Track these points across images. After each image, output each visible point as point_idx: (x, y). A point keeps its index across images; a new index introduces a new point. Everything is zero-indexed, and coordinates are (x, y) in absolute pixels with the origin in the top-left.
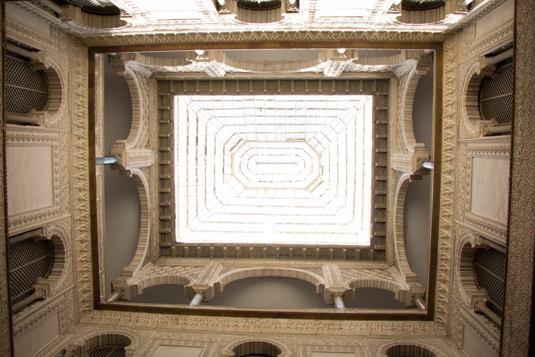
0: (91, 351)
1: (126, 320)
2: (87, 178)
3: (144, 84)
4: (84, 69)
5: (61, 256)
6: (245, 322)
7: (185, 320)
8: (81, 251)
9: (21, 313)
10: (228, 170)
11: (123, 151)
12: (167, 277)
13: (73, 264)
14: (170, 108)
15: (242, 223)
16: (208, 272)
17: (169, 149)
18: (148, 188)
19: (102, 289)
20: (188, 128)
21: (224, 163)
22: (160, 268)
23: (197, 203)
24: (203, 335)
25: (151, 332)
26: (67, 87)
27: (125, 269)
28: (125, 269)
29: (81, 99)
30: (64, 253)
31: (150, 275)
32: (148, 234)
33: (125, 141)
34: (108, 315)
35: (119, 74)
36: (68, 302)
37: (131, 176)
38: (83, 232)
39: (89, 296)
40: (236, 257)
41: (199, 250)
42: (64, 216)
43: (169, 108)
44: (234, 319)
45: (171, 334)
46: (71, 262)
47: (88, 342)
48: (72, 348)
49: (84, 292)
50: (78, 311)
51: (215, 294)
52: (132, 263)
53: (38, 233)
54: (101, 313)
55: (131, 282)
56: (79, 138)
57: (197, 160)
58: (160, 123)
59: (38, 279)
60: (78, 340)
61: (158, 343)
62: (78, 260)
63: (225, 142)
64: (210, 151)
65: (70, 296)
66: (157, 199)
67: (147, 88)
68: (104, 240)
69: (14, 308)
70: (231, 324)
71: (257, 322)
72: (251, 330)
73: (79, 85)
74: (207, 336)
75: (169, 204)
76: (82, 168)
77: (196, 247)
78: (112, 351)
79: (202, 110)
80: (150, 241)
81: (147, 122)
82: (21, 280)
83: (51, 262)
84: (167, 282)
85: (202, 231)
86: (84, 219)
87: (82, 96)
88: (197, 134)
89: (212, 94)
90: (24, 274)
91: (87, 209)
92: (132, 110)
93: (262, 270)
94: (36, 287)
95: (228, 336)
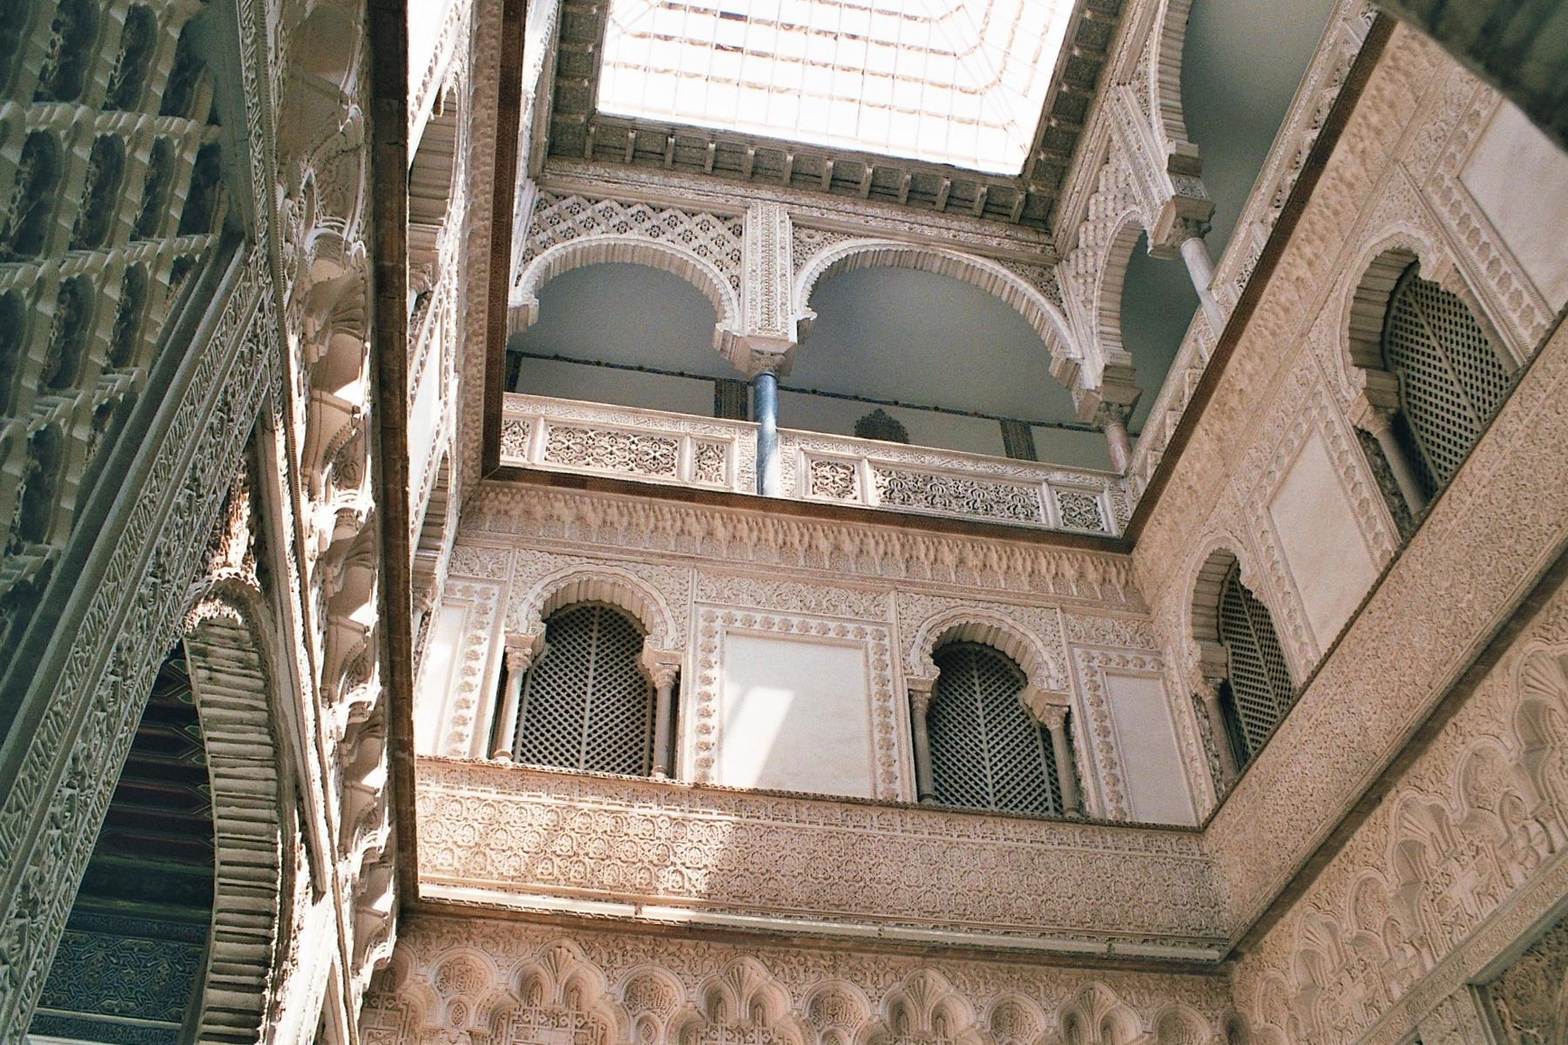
12: (1109, 264)
14: (633, 129)
18: (852, 242)
23: (920, 49)
27: (1054, 369)
28: (1054, 369)
33: (720, 327)
34: (1154, 535)
37: (814, 316)
41: (1059, 125)
42: (892, 616)
43: (632, 135)
47: (1199, 630)
53: (921, 706)
55: (1091, 377)
77: (1049, 128)
80: (998, 260)
83: (991, 654)
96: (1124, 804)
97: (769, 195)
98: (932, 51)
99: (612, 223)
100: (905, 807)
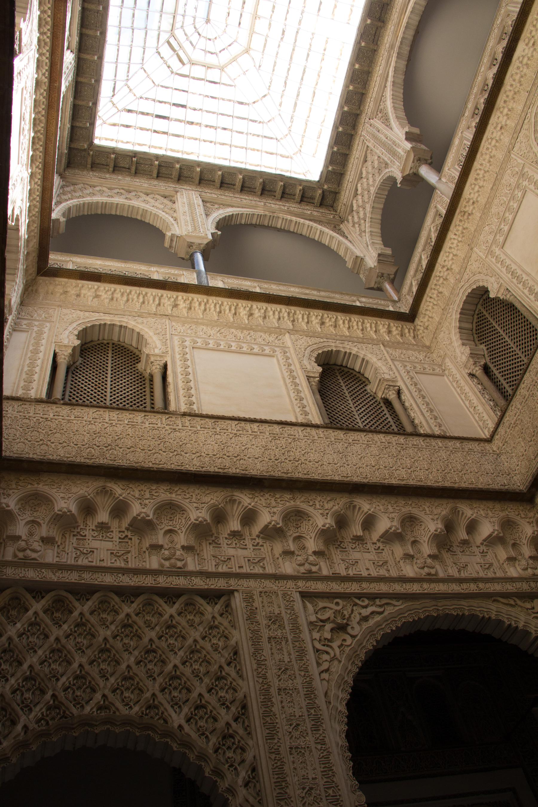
0: (476, 340)
1: (443, 283)
2: (235, 301)
3: (75, 192)
4: (73, 286)
5: (342, 355)
6: (501, 113)
7: (468, 202)
8: (335, 326)
9: (416, 421)
10: (213, 74)
11: (184, 240)
12: (373, 207)
13: (353, 342)
14: (113, 153)
15: (304, 70)
16: (383, 145)
17: (178, 166)
19: (380, 305)
20: (141, 129)
21: (202, 79)
22: (355, 214)
23: (258, 136)
24: (503, 181)
25: (474, 256)
26: (102, 314)
27: (349, 265)
28: (349, 265)
29: (117, 295)
30: (338, 352)
31: (365, 232)
32: (302, 221)
33: (169, 234)
35: (62, 229)
36: (402, 356)
37: (219, 233)
38: (310, 319)
39: (395, 326)
40: (363, 94)
41: (338, 150)
42: (289, 343)
43: (113, 156)
44: (490, 128)
45: (487, 228)
46: (350, 343)
48: (469, 365)
49: (389, 332)
50: (414, 345)
51: (420, 142)
52: (341, 253)
54: (422, 316)
55: (371, 261)
56: (176, 306)
57: (192, 123)
58: (136, 173)
59: (369, 391)
60: (460, 355)
61: (497, 251)
62: (348, 334)
63: (168, 71)
64: (180, 98)
65: (397, 353)
66: (251, 198)
67: (80, 186)
68: (314, 290)
69: (409, 429)
70: (497, 135)
71: (508, 93)
72: (519, 107)
73: (97, 296)
74: (506, 177)
75: (261, 180)
76: (220, 307)
77: (333, 153)
78: (485, 313)
79: (115, 99)
80: (310, 220)
81: (134, 194)
82: (371, 413)
84: (379, 208)
85: (303, 136)
86: (291, 315)
87: (113, 294)
88: (152, 115)
89: (98, 81)
90: (363, 409)
91: (279, 310)
92: (116, 215)
93: (397, 57)
94: (380, 395)
95: (517, 145)
96: (443, 428)
97: (188, 188)
98: (265, 137)
99: (102, 193)
100: (317, 426)
